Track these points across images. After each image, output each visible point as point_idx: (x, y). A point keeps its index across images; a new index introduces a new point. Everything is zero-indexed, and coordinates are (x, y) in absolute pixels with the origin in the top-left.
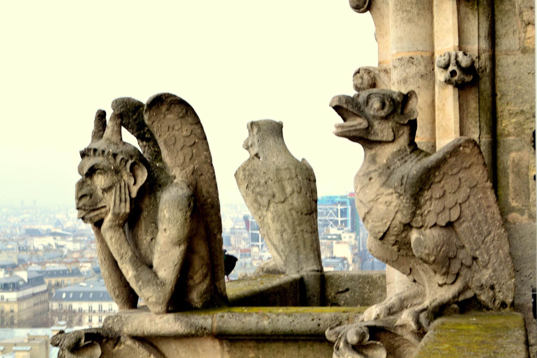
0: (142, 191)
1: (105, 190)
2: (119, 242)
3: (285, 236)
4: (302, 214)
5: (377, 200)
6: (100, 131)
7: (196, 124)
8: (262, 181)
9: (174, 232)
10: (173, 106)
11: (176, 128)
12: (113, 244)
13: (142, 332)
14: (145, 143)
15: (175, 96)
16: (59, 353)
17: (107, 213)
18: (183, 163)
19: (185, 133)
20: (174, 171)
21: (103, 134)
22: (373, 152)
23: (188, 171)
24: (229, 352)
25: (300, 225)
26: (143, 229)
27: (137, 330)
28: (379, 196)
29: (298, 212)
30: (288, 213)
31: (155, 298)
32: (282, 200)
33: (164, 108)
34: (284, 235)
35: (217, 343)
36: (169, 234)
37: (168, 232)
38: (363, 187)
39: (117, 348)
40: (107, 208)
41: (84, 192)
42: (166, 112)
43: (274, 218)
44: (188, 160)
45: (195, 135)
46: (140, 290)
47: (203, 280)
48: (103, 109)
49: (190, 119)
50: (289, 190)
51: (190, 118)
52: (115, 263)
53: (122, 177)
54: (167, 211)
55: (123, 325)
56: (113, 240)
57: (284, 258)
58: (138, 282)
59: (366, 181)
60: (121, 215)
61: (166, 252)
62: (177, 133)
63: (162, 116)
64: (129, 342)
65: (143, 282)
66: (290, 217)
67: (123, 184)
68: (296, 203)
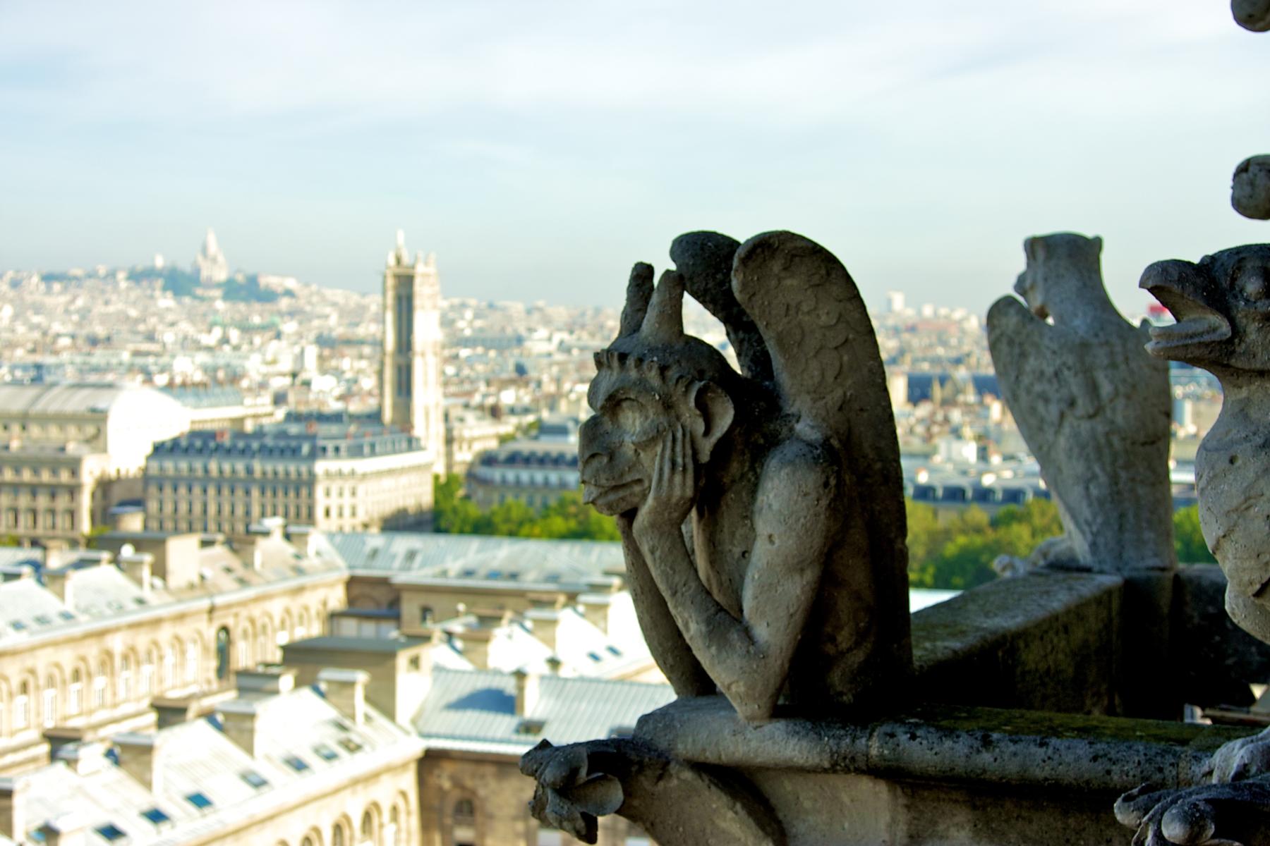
0: (724, 448)
3: (1094, 491)
4: (1133, 443)
5: (1247, 509)
6: (639, 310)
7: (849, 300)
8: (1049, 371)
9: (791, 542)
10: (797, 259)
11: (805, 308)
14: (741, 335)
17: (644, 497)
18: (820, 383)
19: (823, 319)
20: (798, 404)
22: (1244, 393)
23: (830, 403)
24: (908, 807)
25: (1128, 466)
26: (726, 530)
27: (704, 750)
28: (1252, 501)
29: (1124, 439)
30: (1103, 441)
32: (1091, 411)
33: (776, 266)
34: (1091, 487)
38: (1215, 476)
39: (661, 784)
40: (646, 484)
42: (783, 274)
43: (1071, 449)
44: (830, 379)
45: (848, 322)
47: (857, 644)
49: (837, 290)
50: (1106, 389)
51: (835, 288)
52: (663, 603)
56: (658, 554)
57: (1089, 537)
59: (1223, 464)
60: (674, 500)
62: (807, 318)
63: (774, 283)
64: (688, 775)
66: (1106, 451)
67: (679, 435)
68: (1119, 419)
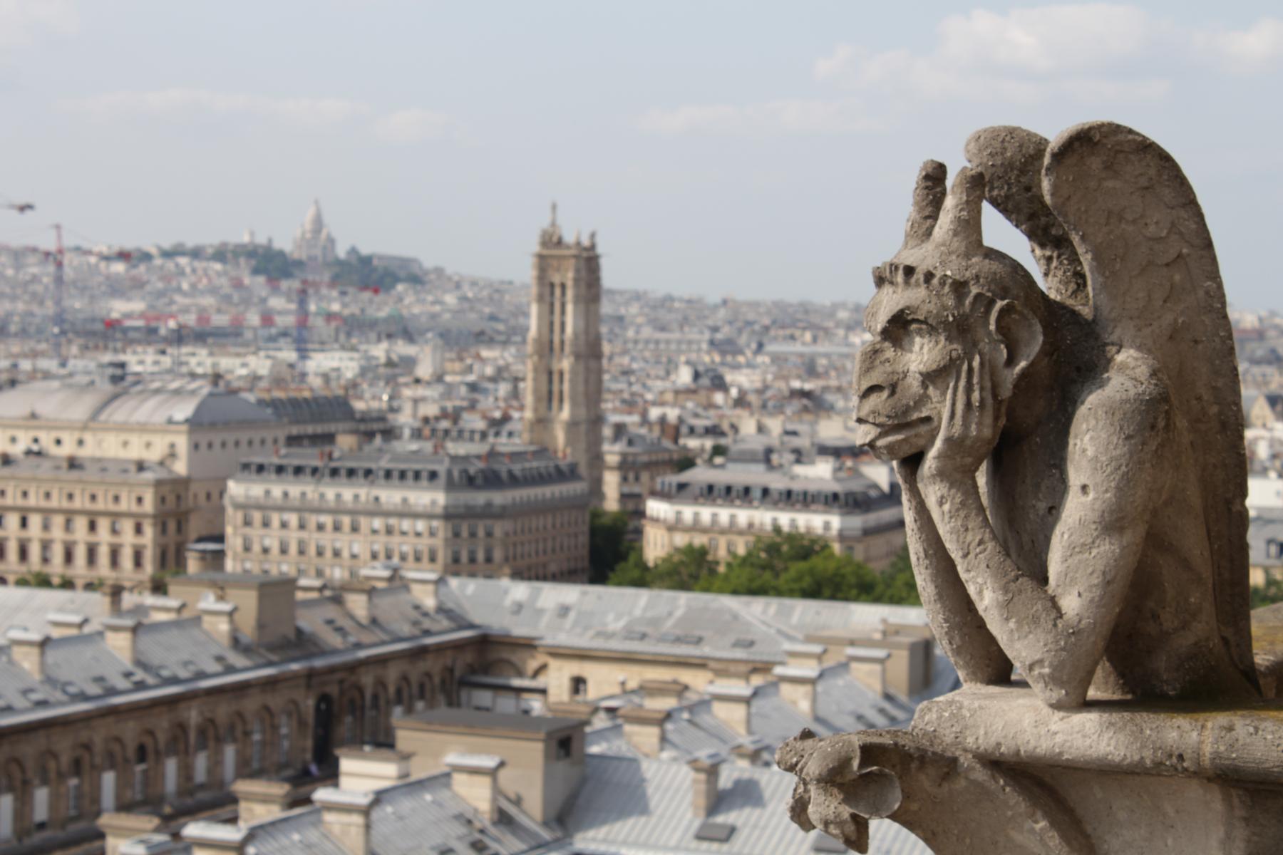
1: (932, 377)
2: (962, 514)
6: (927, 218)
7: (1184, 206)
12: (947, 517)
13: (1013, 748)
15: (1131, 131)
16: (795, 790)
21: (933, 226)
24: (1246, 820)
31: (1051, 665)
35: (1216, 799)
36: (1095, 499)
37: (1091, 495)
41: (875, 378)
45: (1181, 234)
46: (1011, 640)
48: (940, 160)
49: (1168, 194)
53: (975, 344)
54: (1091, 438)
55: (966, 727)
56: (946, 507)
58: (1007, 619)
60: (968, 442)
61: (1084, 545)
62: (1131, 228)
65: (1019, 622)
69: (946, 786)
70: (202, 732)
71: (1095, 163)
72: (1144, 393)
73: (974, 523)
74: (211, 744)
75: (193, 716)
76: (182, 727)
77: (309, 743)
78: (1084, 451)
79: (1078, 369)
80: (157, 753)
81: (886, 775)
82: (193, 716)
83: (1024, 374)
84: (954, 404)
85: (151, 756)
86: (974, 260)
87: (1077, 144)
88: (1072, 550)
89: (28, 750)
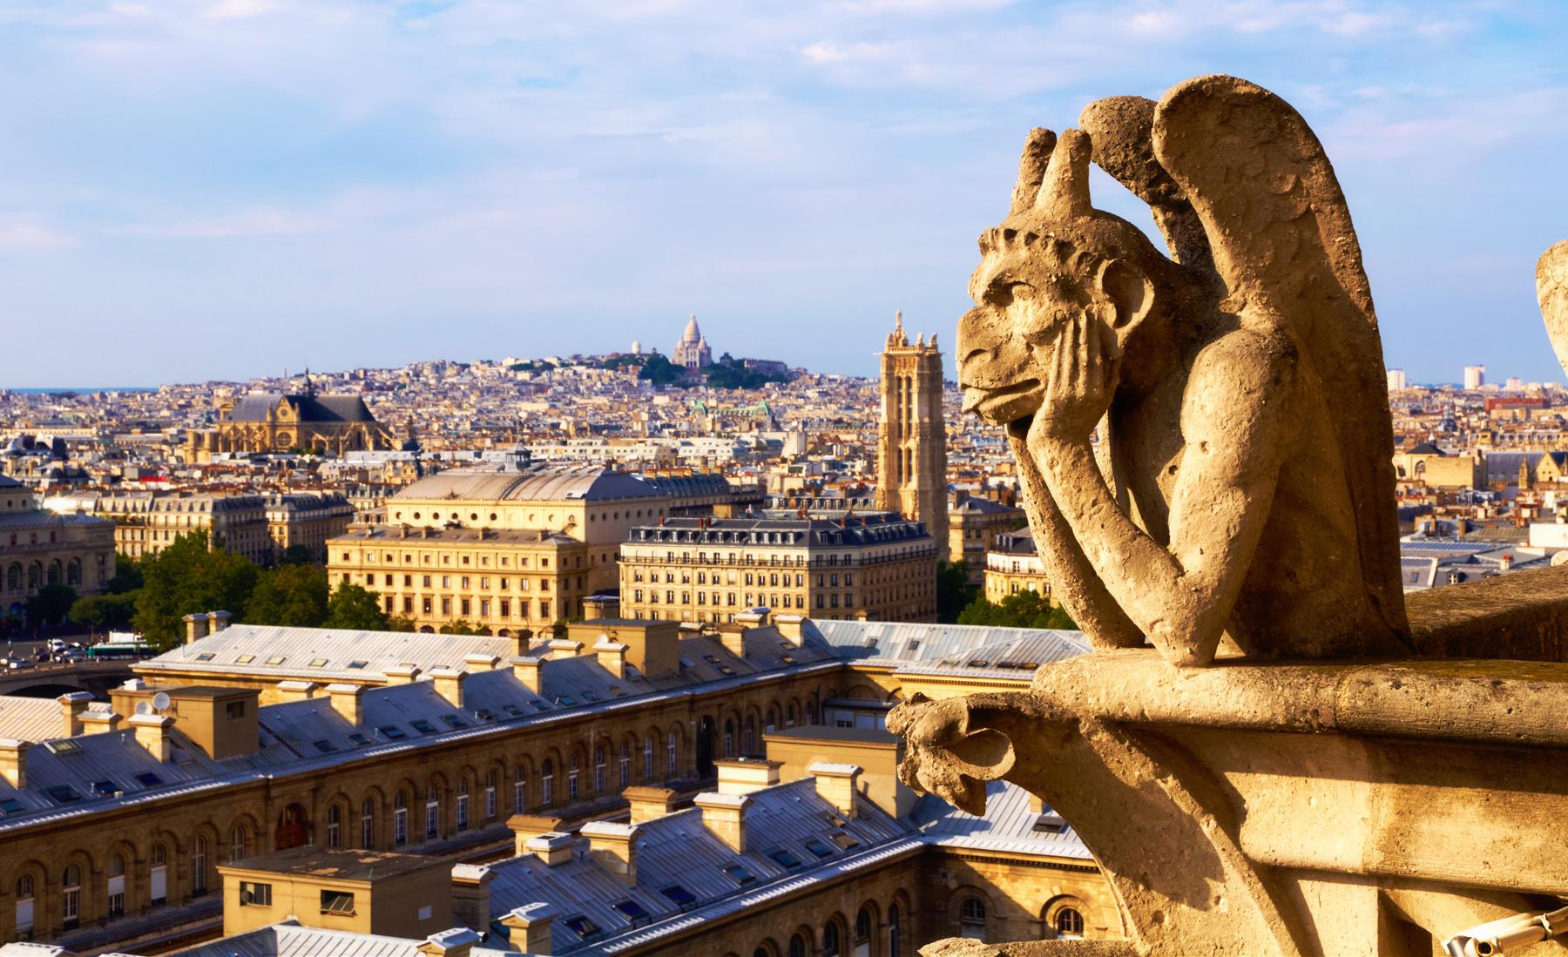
2: (1074, 475)
11: (1250, 172)
12: (1058, 478)
31: (1173, 623)
58: (1124, 578)
69: (1068, 748)
70: (600, 748)
71: (1210, 120)
72: (1267, 347)
73: (1088, 483)
74: (609, 757)
75: (592, 735)
76: (583, 745)
77: (694, 756)
78: (1202, 407)
79: (1198, 328)
80: (562, 766)
81: (999, 737)
82: (592, 735)
83: (1136, 330)
84: (1060, 365)
85: (557, 769)
86: (1081, 221)
87: (1187, 99)
88: (1193, 508)
89: (451, 765)
